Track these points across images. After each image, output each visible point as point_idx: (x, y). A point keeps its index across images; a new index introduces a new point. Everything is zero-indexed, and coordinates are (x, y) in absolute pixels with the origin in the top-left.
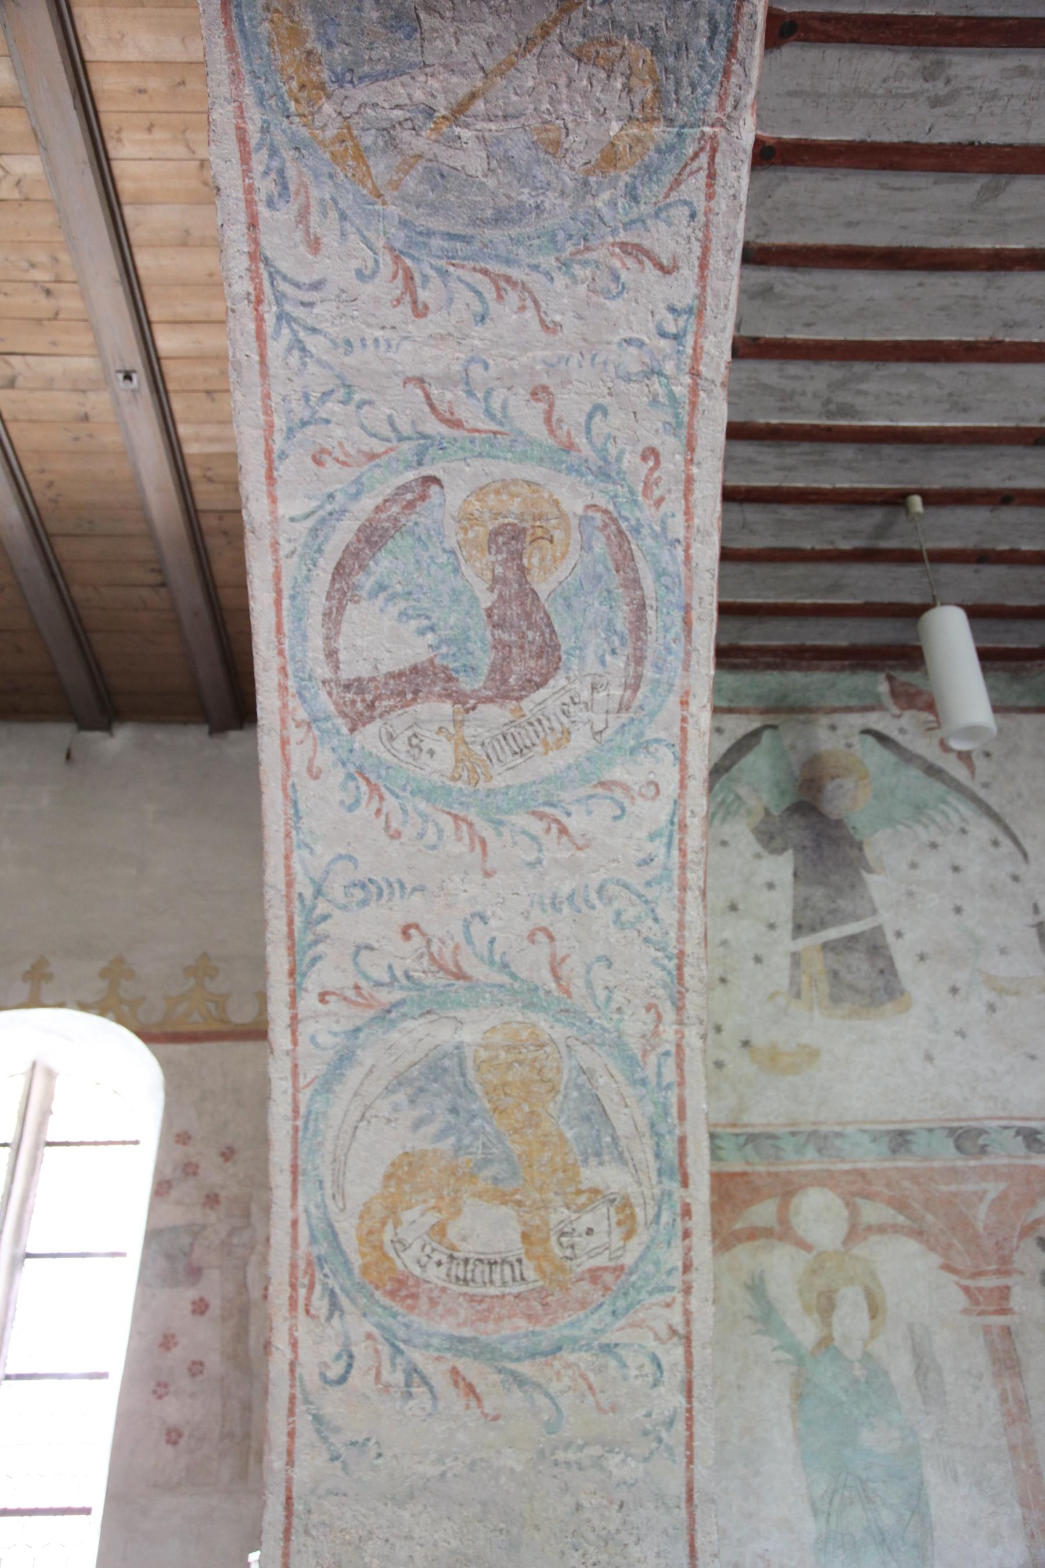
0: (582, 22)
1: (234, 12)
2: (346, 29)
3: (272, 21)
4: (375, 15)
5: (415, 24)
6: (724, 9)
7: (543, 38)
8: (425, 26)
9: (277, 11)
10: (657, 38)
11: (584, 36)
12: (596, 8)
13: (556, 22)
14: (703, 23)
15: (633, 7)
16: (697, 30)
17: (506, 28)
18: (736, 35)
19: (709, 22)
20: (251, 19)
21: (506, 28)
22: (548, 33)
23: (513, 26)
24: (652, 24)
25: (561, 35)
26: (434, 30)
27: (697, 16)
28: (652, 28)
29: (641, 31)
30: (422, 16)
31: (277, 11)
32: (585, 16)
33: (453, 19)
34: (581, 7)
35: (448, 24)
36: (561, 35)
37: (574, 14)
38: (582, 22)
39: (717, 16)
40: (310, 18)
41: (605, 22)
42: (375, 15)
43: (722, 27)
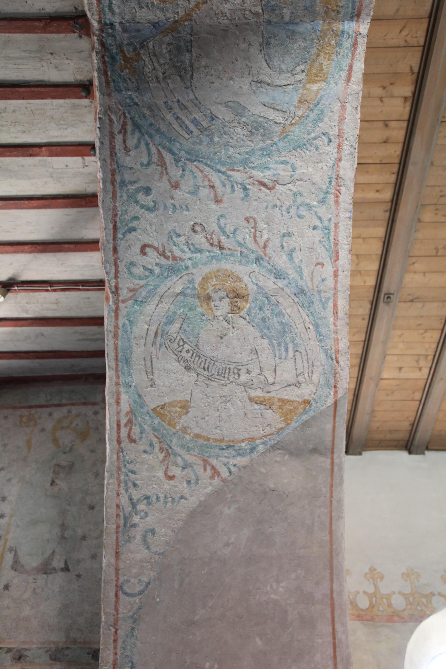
0: (179, 10)
1: (356, 11)
2: (300, 5)
3: (337, 6)
4: (285, 11)
5: (264, 8)
6: (108, 17)
7: (199, 3)
8: (259, 7)
9: (334, 11)
10: (139, 4)
11: (177, 4)
12: (172, 16)
13: (193, 10)
14: (117, 11)
15: (154, 17)
16: (119, 7)
17: (218, 7)
18: (98, 6)
19: (114, 11)
20: (348, 8)
21: (218, 7)
22: (196, 5)
23: (215, 8)
24: (143, 10)
25: (189, 4)
26: (256, 6)
27: (120, 14)
28: (143, 8)
29: (148, 6)
30: (261, 11)
31: (334, 11)
32: (178, 13)
33: (245, 10)
34: (180, 16)
35: (248, 8)
36: (189, 4)
37: (184, 13)
38: (179, 10)
39: (110, 14)
40: (317, 9)
41: (167, 10)
42: (285, 11)
43: (107, 9)
